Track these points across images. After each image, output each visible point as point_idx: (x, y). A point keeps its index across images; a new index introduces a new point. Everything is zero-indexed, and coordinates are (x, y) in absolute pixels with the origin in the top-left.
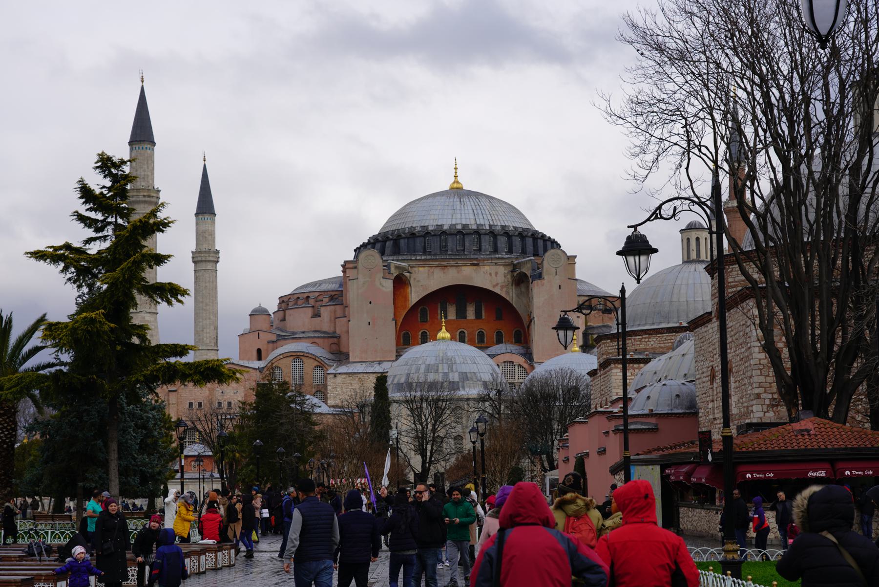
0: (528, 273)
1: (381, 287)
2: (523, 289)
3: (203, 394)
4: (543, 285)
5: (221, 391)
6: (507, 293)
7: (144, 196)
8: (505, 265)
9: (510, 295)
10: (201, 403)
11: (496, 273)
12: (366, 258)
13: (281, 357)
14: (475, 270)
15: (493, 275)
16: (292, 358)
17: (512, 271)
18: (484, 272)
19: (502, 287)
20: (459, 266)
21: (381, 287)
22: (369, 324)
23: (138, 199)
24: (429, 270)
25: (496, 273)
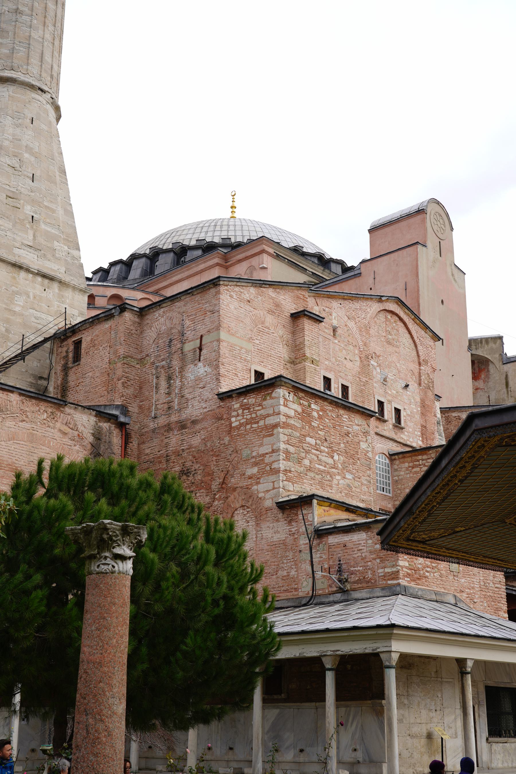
1: (453, 282)
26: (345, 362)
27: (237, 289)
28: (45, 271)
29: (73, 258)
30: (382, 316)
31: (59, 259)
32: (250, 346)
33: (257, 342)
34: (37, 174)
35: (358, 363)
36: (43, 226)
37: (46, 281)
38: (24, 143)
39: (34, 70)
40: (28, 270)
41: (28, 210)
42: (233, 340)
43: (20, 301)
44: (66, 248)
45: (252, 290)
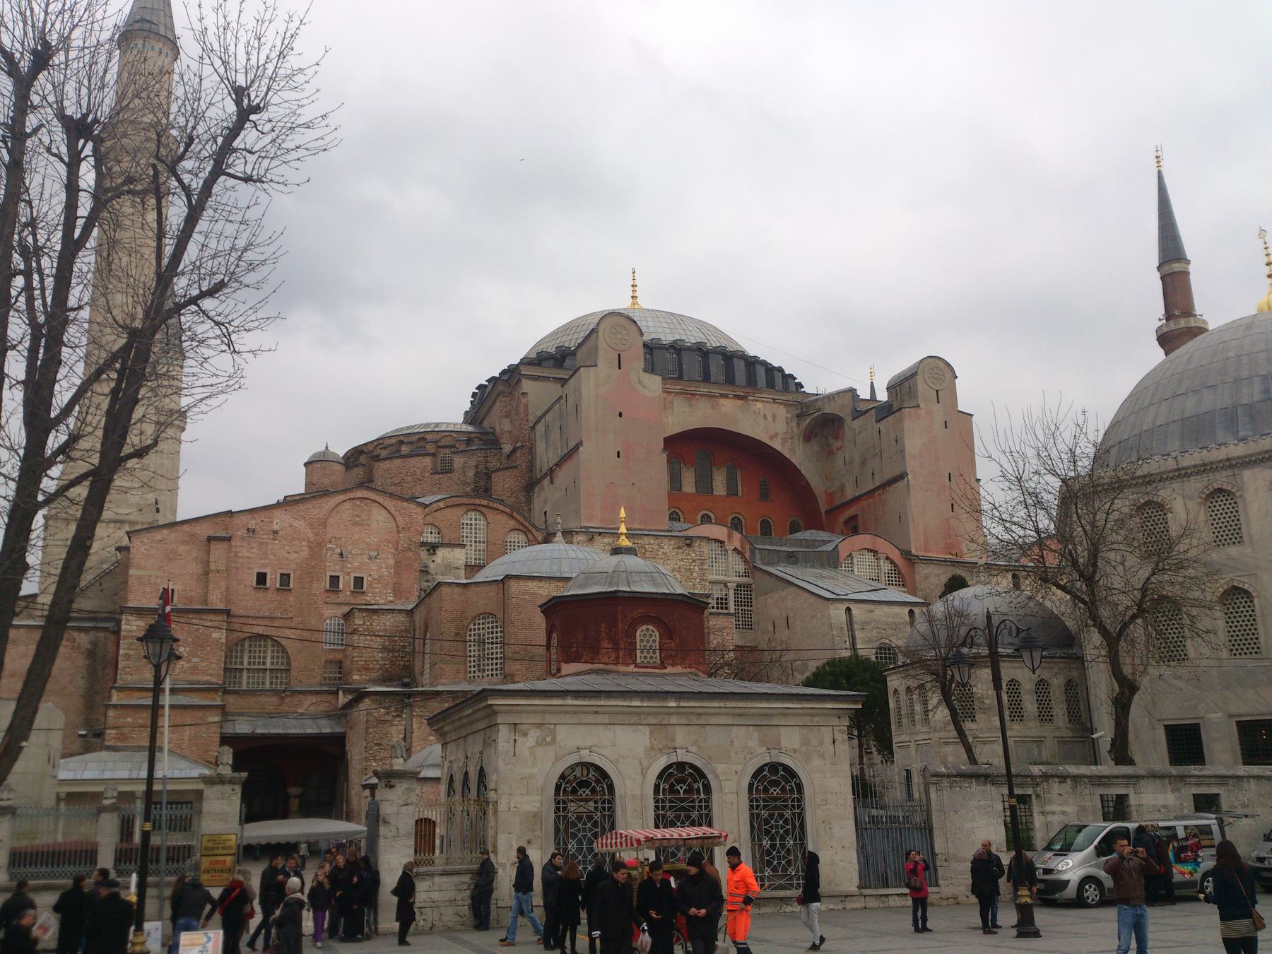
0: (846, 414)
1: (640, 389)
2: (816, 448)
3: (294, 556)
4: (918, 418)
5: (338, 551)
6: (791, 450)
8: (787, 404)
9: (799, 455)
11: (774, 417)
12: (614, 331)
13: (441, 505)
15: (770, 418)
16: (463, 509)
19: (784, 441)
20: (714, 396)
21: (640, 389)
22: (618, 456)
25: (774, 417)
27: (149, 535)
30: (348, 505)
32: (159, 573)
33: (168, 568)
35: (306, 553)
37: (119, 524)
42: (141, 573)
45: (165, 531)
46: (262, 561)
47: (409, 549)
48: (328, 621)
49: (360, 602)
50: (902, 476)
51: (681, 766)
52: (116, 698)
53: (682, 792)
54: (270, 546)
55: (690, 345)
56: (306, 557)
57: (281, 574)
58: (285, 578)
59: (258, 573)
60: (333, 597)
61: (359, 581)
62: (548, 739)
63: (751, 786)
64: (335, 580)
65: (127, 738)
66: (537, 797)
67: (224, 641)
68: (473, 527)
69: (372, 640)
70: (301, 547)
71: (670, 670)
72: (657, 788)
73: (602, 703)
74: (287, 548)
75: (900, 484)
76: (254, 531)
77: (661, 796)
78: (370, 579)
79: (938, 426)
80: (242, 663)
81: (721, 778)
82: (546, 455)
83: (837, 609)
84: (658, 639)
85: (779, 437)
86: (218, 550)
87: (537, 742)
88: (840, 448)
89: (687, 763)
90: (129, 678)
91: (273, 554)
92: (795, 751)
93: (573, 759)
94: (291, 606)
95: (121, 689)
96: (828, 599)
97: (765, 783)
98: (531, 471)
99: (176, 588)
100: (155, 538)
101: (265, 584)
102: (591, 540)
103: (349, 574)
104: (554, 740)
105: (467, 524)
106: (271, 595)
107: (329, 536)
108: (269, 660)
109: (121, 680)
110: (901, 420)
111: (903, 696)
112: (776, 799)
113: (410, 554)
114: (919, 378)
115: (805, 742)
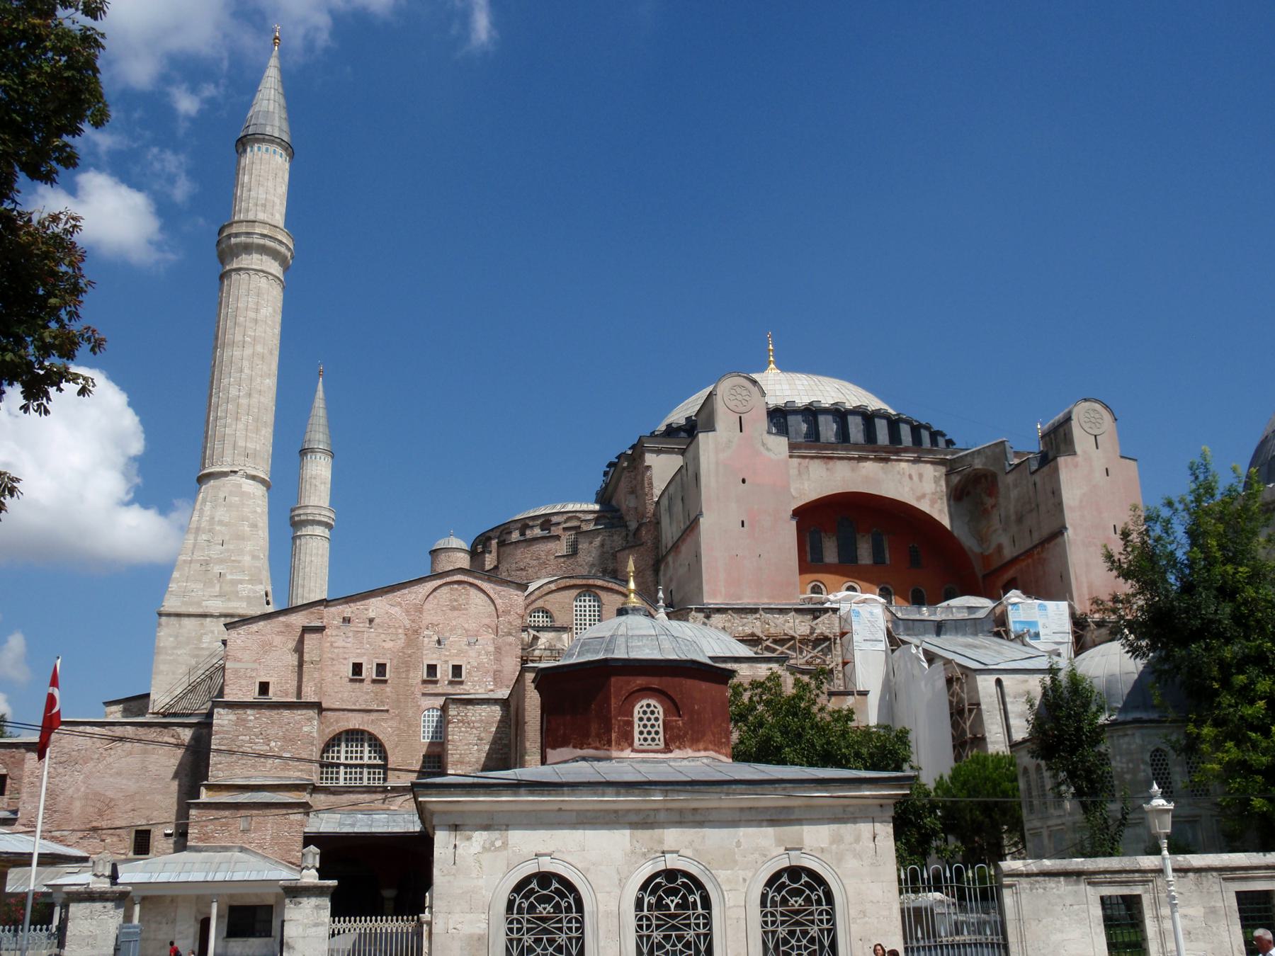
3: (389, 645)
4: (1076, 466)
7: (264, 236)
10: (385, 665)
11: (921, 476)
12: (733, 392)
13: (553, 587)
14: (883, 468)
15: (915, 478)
17: (948, 475)
18: (899, 473)
19: (933, 502)
22: (743, 526)
23: (249, 240)
24: (800, 464)
25: (921, 476)
26: (384, 644)
28: (225, 611)
29: (255, 592)
30: (445, 590)
31: (242, 598)
32: (256, 666)
34: (226, 538)
35: (403, 641)
36: (229, 577)
38: (216, 519)
39: (228, 459)
40: (212, 616)
41: (217, 569)
42: (238, 665)
43: (206, 639)
44: (250, 586)
45: (262, 623)
46: (359, 651)
47: (510, 634)
48: (426, 712)
49: (458, 691)
50: (1060, 531)
51: (671, 874)
52: (205, 796)
53: (672, 906)
54: (366, 635)
55: (827, 405)
56: (403, 645)
57: (378, 665)
58: (381, 668)
59: (354, 664)
60: (431, 689)
61: (457, 670)
62: (498, 843)
63: (764, 897)
64: (432, 669)
65: (209, 837)
66: (483, 916)
67: (315, 735)
68: (587, 609)
69: (467, 732)
70: (397, 634)
71: (677, 753)
72: (639, 904)
73: (567, 799)
74: (383, 636)
75: (1059, 540)
76: (349, 621)
77: (645, 912)
78: (469, 667)
79: (1099, 474)
80: (338, 758)
81: (723, 888)
82: (670, 532)
83: (986, 680)
84: (661, 717)
85: (928, 497)
86: (310, 640)
87: (484, 848)
88: (993, 507)
89: (679, 871)
90: (221, 774)
91: (368, 643)
92: (822, 850)
93: (531, 869)
94: (388, 697)
95: (210, 788)
96: (976, 670)
97: (784, 893)
98: (657, 548)
99: (272, 680)
100: (251, 630)
101: (361, 675)
102: (708, 617)
103: (446, 662)
104: (505, 844)
105: (580, 606)
106: (367, 686)
107: (425, 622)
108: (366, 755)
109: (212, 776)
110: (1056, 471)
111: (1033, 776)
112: (797, 912)
113: (511, 639)
114: (1074, 423)
115: (837, 840)
